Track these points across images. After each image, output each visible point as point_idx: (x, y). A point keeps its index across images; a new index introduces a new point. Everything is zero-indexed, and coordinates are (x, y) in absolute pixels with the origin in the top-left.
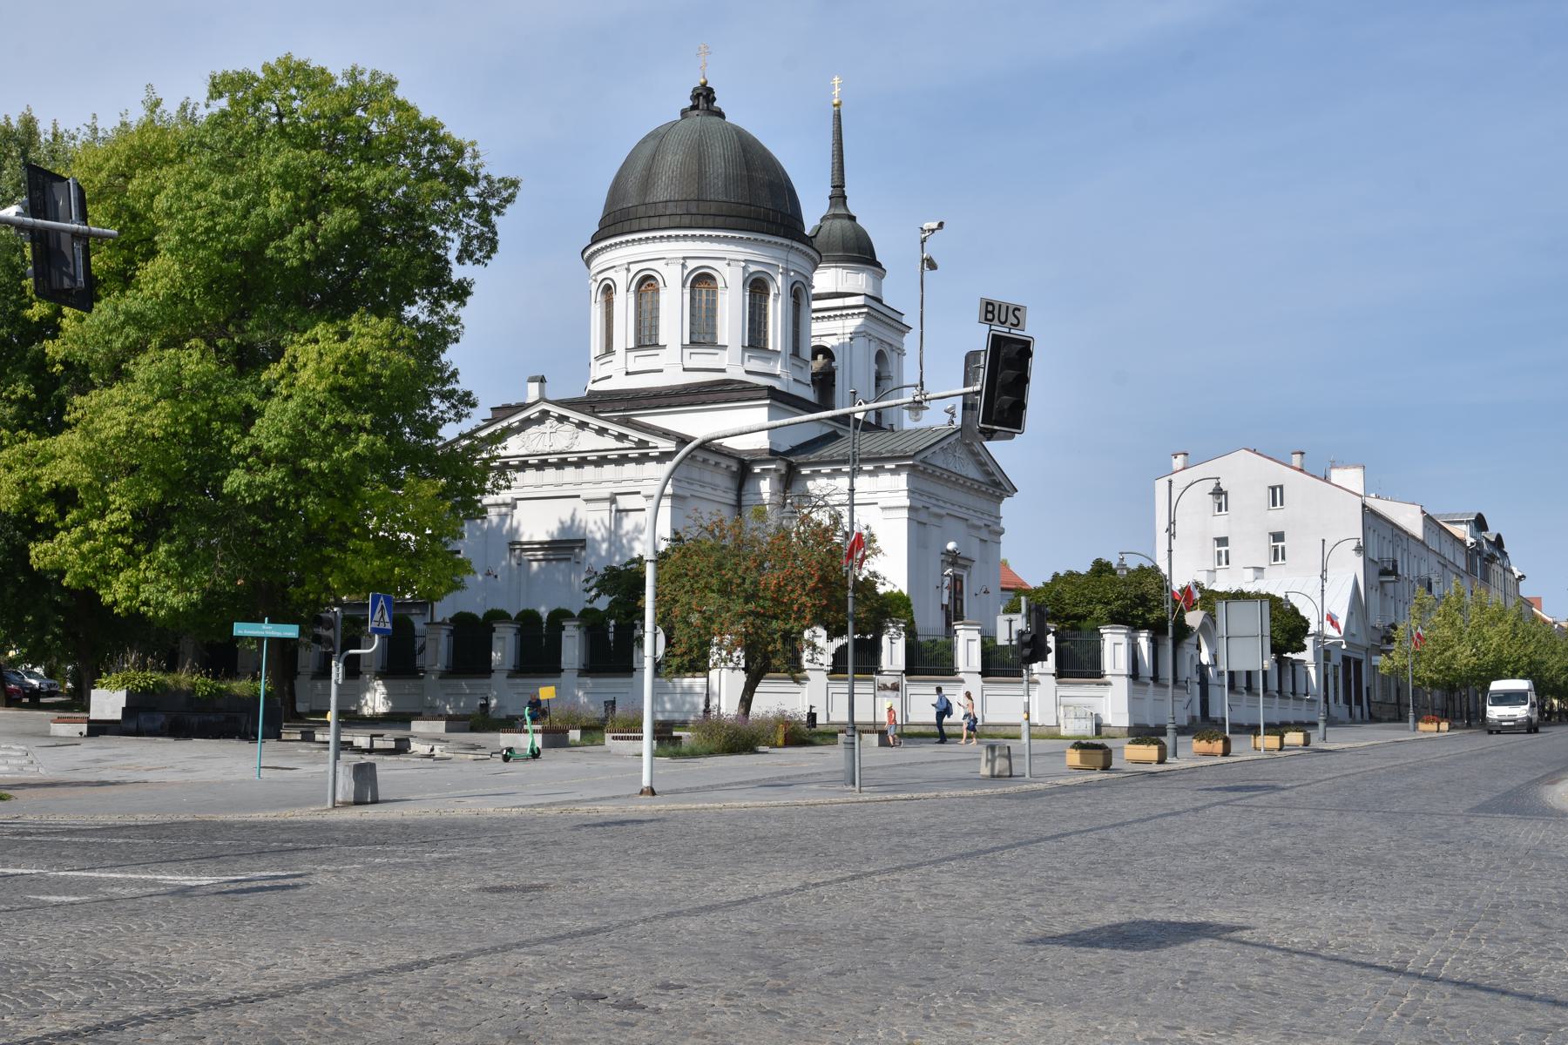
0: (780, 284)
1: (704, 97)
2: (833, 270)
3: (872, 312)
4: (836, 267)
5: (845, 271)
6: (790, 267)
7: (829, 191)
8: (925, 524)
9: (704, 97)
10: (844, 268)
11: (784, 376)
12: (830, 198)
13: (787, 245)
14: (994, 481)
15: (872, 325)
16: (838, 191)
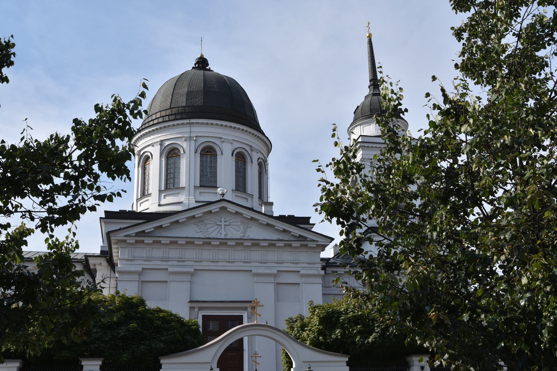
0: (185, 146)
1: (202, 63)
2: (356, 128)
3: (366, 145)
4: (356, 126)
5: (362, 127)
6: (192, 135)
7: (368, 83)
8: (167, 282)
9: (202, 63)
10: (361, 125)
11: (186, 202)
12: (369, 88)
13: (187, 123)
14: (293, 236)
15: (367, 152)
16: (372, 83)
